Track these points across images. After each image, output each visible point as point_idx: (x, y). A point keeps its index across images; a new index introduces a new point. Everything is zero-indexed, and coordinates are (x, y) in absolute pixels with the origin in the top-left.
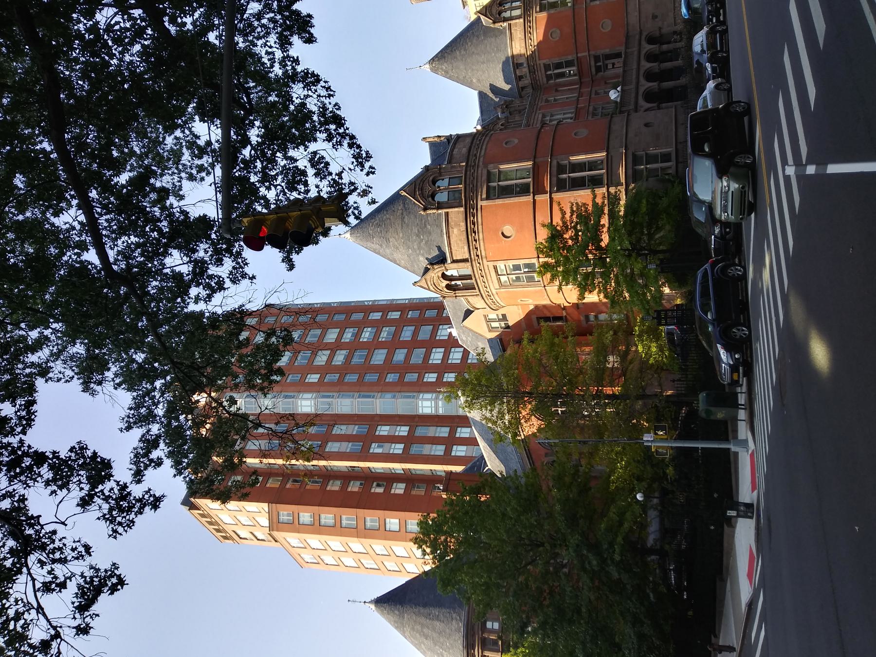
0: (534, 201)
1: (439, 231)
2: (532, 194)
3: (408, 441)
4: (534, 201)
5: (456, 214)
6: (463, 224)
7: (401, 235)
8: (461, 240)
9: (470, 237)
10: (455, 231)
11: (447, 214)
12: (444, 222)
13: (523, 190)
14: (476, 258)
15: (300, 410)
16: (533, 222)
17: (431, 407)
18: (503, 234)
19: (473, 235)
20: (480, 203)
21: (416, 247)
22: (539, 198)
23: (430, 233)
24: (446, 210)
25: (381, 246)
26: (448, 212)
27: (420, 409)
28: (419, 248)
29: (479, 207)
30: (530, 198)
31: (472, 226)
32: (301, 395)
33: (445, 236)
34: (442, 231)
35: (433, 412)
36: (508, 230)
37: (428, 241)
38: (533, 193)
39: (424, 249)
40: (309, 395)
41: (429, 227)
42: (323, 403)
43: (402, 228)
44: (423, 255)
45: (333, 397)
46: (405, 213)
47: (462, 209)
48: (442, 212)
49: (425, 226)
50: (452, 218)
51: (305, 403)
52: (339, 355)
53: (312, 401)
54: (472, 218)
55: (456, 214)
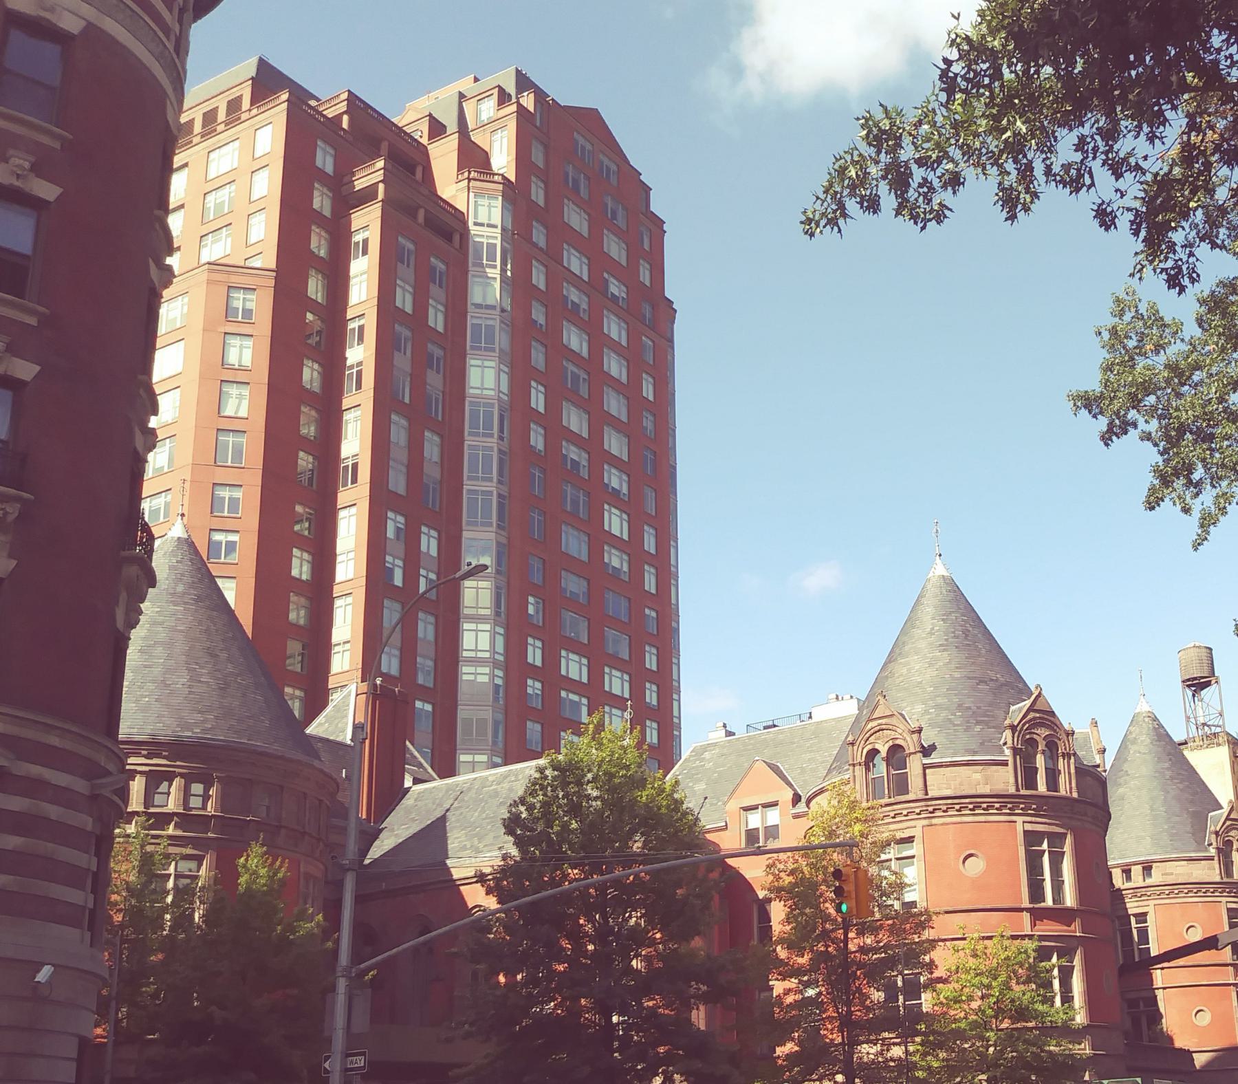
0: (1021, 910)
1: (973, 747)
2: (1031, 906)
3: (409, 597)
4: (1021, 910)
5: (1005, 780)
6: (986, 790)
7: (957, 675)
8: (961, 784)
9: (967, 800)
10: (977, 776)
11: (1005, 763)
12: (993, 758)
13: (1036, 892)
14: (931, 809)
15: (473, 362)
16: (988, 907)
17: (476, 650)
18: (971, 855)
19: (971, 806)
20: (1019, 819)
21: (940, 700)
22: (1026, 917)
23: (966, 730)
24: (1011, 763)
25: (931, 633)
26: (1007, 765)
27: (473, 626)
28: (937, 706)
29: (1014, 818)
30: (1026, 904)
31: (984, 806)
32: (506, 369)
33: (970, 758)
34: (975, 753)
35: (465, 654)
36: (976, 867)
37: (955, 725)
38: (1033, 908)
39: (938, 715)
40: (505, 388)
41: (978, 728)
42: (488, 415)
43: (969, 678)
44: (926, 712)
45: (501, 438)
46: (992, 684)
47: (1012, 790)
48: (1008, 752)
49: (978, 723)
50: (997, 771)
51: (490, 375)
52: (620, 478)
53: (492, 393)
54: (997, 805)
55: (1005, 780)
